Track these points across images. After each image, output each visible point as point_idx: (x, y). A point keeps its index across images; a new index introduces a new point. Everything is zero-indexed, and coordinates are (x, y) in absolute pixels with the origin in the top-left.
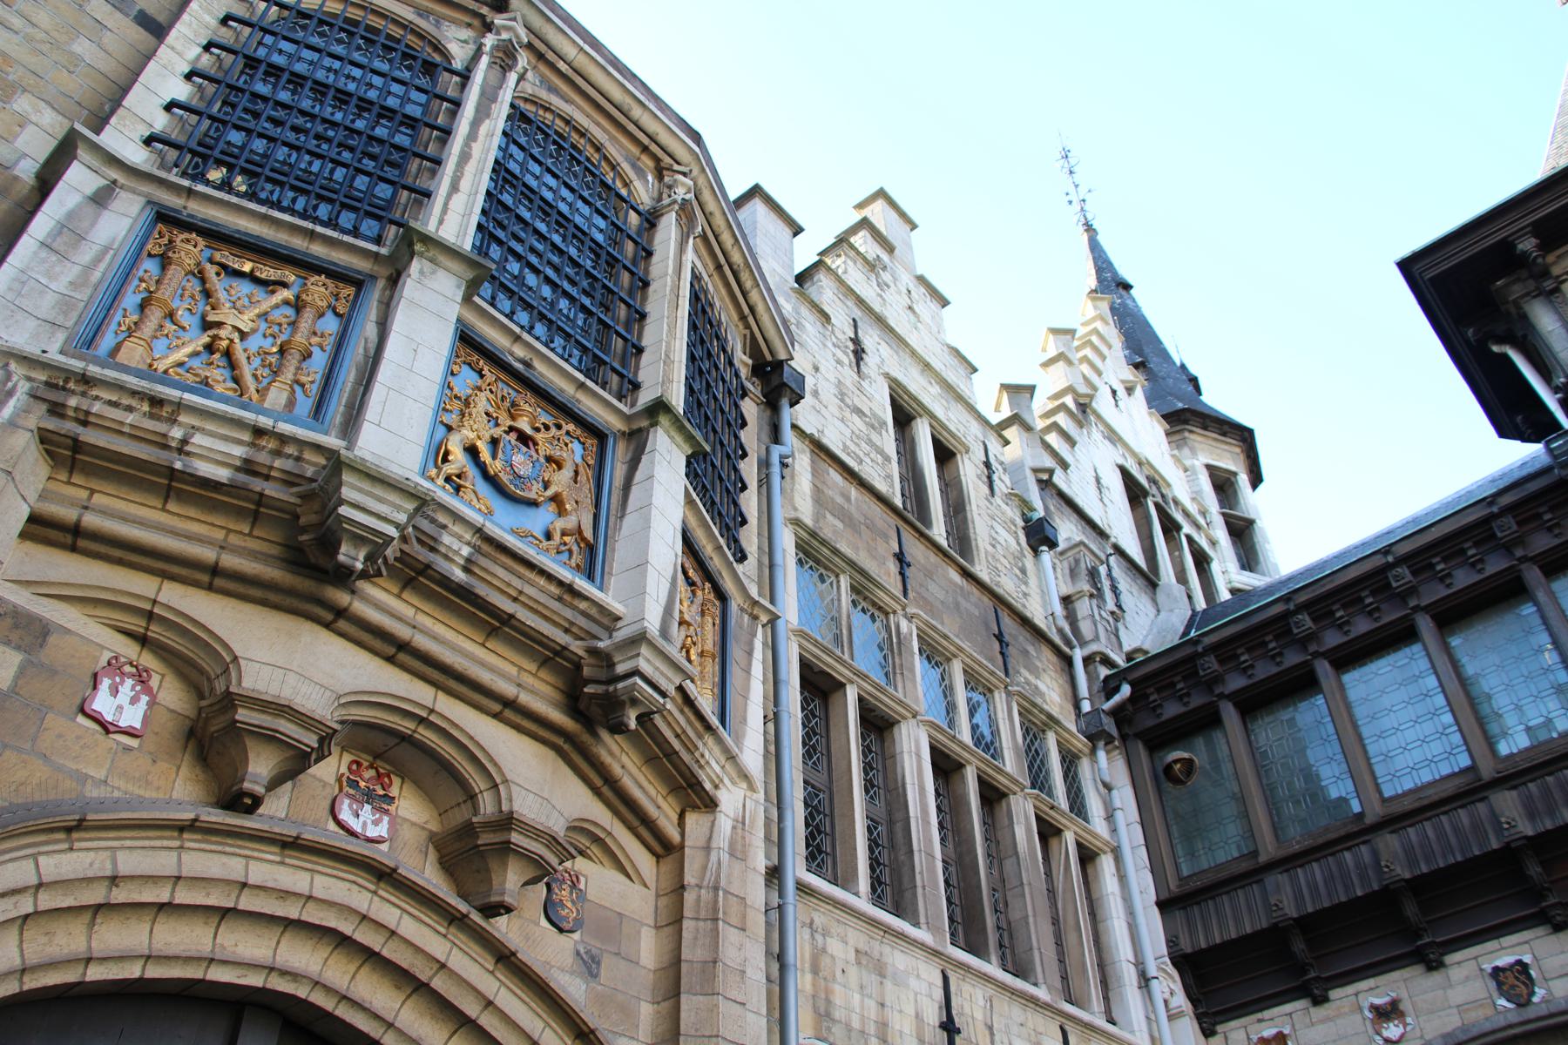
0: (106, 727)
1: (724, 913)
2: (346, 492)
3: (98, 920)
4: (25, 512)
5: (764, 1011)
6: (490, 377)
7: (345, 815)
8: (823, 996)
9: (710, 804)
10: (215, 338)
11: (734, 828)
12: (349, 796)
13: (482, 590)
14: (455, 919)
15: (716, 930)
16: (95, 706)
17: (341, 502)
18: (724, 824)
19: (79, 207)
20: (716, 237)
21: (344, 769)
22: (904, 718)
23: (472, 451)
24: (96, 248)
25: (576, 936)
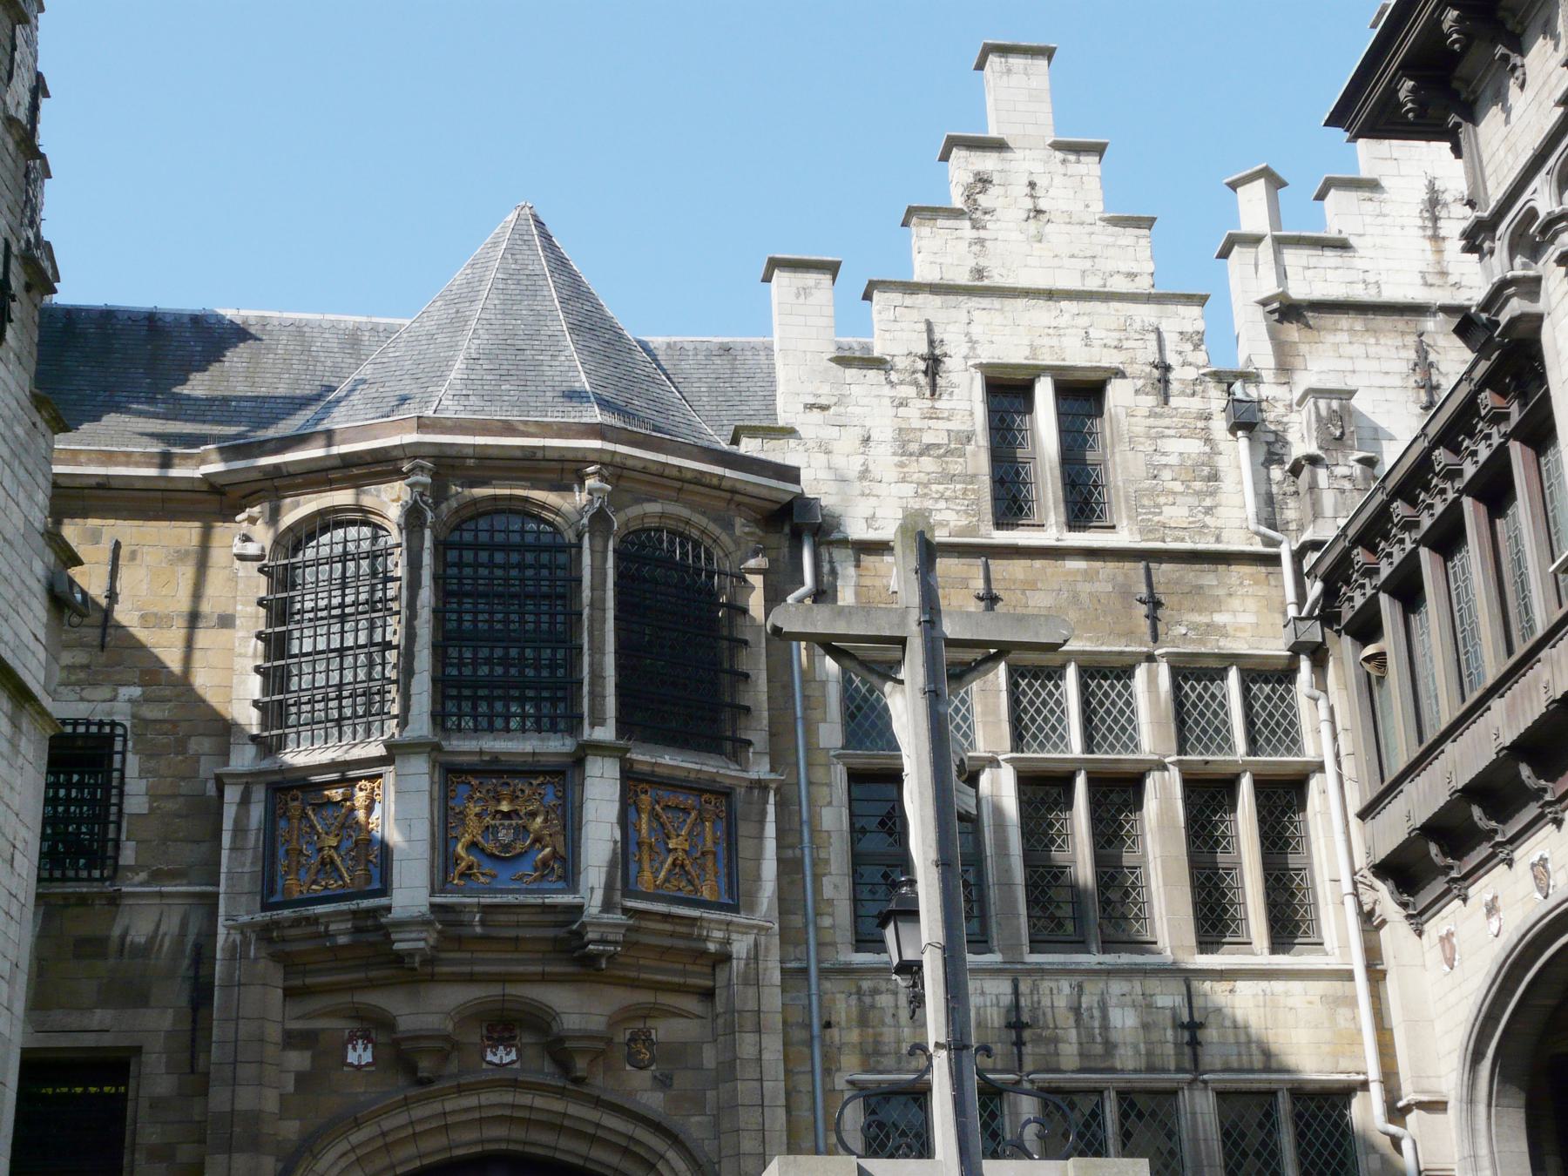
0: (359, 1067)
1: (741, 1026)
2: (394, 937)
3: (717, 970)
4: (280, 992)
5: (782, 1077)
6: (474, 782)
7: (490, 1057)
8: (871, 1040)
9: (725, 958)
10: (323, 858)
11: (747, 965)
12: (489, 1046)
13: (495, 932)
14: (561, 1093)
15: (734, 1040)
16: (349, 1061)
17: (394, 942)
18: (737, 966)
19: (237, 814)
20: (661, 476)
21: (485, 1032)
22: (983, 768)
23: (473, 846)
24: (254, 832)
25: (653, 1068)
